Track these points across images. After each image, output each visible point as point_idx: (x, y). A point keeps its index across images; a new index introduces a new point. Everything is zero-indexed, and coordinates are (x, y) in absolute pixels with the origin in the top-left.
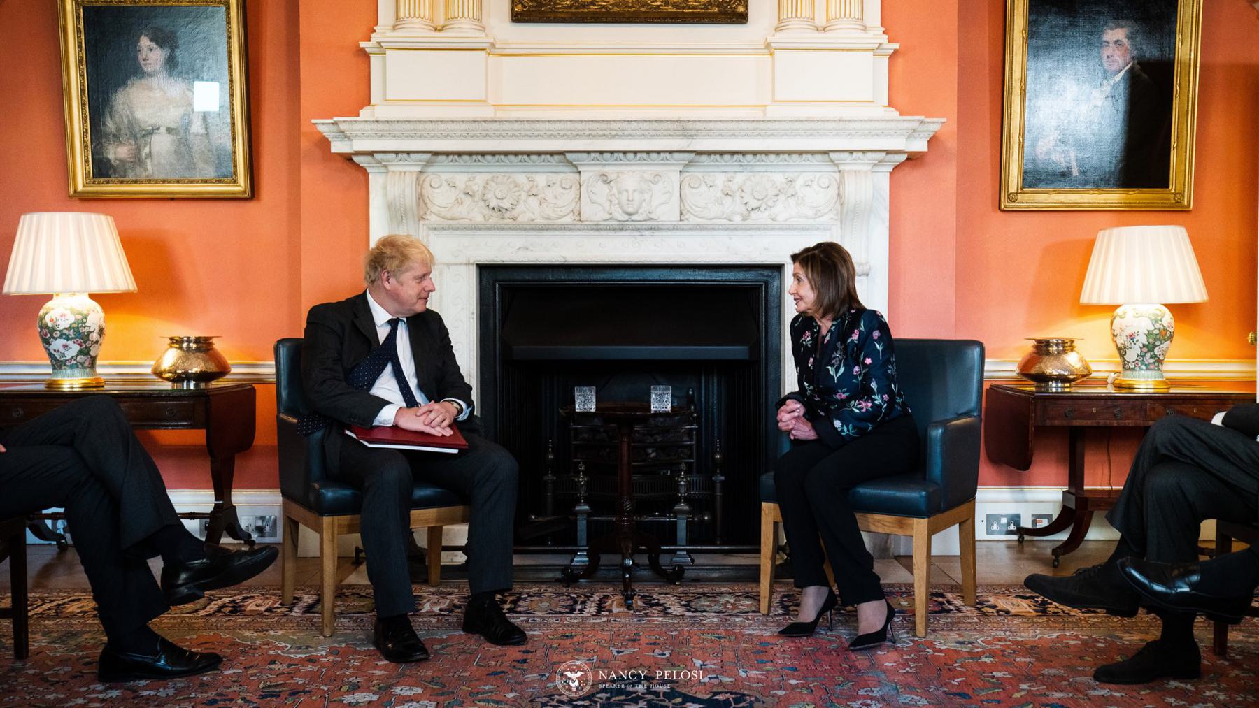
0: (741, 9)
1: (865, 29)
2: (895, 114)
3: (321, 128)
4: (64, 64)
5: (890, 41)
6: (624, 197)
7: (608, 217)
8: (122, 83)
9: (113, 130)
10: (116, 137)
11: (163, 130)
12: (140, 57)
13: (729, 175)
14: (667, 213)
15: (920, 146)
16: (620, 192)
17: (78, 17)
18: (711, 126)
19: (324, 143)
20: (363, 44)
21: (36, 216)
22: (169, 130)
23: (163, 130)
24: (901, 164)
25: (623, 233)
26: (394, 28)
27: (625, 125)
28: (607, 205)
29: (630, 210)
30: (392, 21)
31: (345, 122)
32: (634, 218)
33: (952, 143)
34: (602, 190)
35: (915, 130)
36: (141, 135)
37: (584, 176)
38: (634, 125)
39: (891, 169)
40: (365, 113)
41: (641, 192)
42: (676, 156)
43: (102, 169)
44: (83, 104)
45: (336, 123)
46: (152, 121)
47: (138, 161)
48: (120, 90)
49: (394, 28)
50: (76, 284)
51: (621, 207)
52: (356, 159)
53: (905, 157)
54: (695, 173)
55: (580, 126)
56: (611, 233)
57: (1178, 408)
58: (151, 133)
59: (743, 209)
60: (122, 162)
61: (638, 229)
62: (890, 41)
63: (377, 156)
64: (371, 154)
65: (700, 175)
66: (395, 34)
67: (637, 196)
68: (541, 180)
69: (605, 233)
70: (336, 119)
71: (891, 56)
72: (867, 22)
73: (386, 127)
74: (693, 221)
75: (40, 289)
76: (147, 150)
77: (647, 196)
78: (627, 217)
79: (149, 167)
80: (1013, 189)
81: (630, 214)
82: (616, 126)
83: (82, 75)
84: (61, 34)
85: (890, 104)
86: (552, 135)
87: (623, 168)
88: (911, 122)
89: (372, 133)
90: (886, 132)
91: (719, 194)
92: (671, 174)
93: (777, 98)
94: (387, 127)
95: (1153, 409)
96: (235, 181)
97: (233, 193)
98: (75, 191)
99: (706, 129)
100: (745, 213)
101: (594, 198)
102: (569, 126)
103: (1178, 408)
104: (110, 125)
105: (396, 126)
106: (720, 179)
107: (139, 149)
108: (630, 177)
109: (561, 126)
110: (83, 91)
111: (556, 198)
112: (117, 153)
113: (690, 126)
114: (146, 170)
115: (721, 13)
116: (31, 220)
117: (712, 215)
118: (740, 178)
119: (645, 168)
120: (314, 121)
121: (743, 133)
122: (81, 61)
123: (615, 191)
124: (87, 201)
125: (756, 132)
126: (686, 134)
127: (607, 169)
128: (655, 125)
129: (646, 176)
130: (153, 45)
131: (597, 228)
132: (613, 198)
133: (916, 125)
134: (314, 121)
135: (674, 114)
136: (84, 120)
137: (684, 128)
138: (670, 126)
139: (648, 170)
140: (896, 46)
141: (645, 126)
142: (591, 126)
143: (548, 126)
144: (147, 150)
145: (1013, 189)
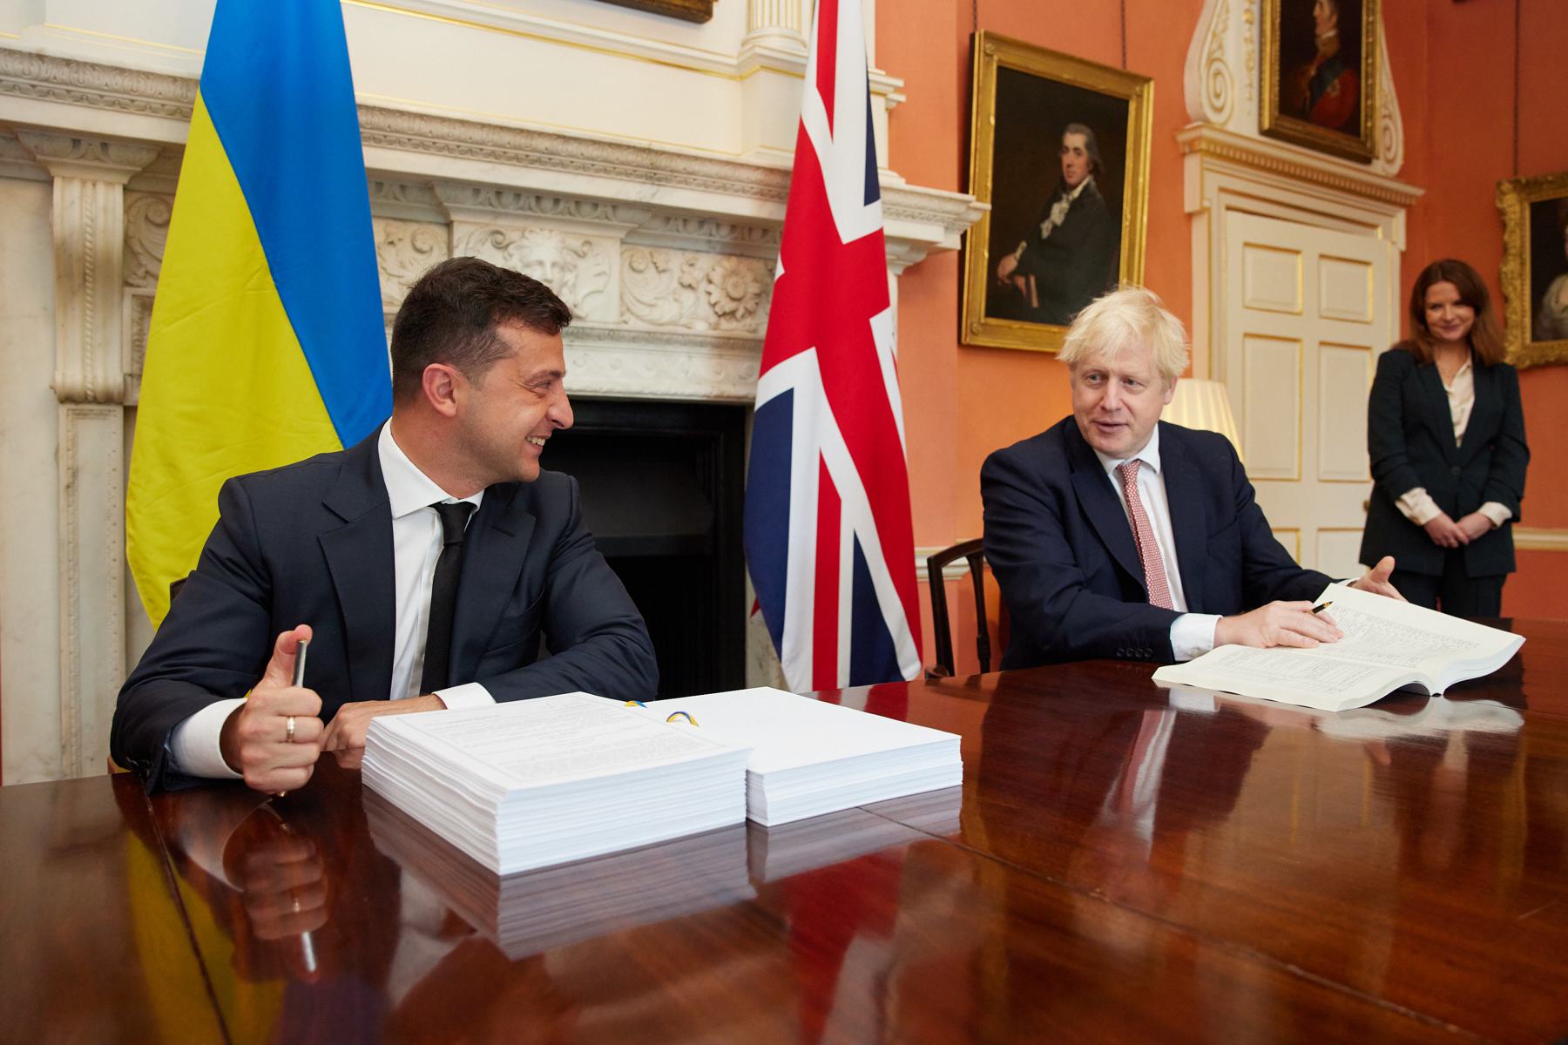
13: (689, 255)
18: (695, 166)
27: (558, 146)
38: (572, 148)
41: (563, 269)
65: (646, 251)
74: (634, 324)
77: (569, 277)
91: (675, 284)
100: (714, 319)
106: (675, 261)
113: (663, 161)
117: (665, 320)
126: (654, 175)
127: (502, 223)
137: (653, 163)
140: (902, 98)
143: (419, 125)
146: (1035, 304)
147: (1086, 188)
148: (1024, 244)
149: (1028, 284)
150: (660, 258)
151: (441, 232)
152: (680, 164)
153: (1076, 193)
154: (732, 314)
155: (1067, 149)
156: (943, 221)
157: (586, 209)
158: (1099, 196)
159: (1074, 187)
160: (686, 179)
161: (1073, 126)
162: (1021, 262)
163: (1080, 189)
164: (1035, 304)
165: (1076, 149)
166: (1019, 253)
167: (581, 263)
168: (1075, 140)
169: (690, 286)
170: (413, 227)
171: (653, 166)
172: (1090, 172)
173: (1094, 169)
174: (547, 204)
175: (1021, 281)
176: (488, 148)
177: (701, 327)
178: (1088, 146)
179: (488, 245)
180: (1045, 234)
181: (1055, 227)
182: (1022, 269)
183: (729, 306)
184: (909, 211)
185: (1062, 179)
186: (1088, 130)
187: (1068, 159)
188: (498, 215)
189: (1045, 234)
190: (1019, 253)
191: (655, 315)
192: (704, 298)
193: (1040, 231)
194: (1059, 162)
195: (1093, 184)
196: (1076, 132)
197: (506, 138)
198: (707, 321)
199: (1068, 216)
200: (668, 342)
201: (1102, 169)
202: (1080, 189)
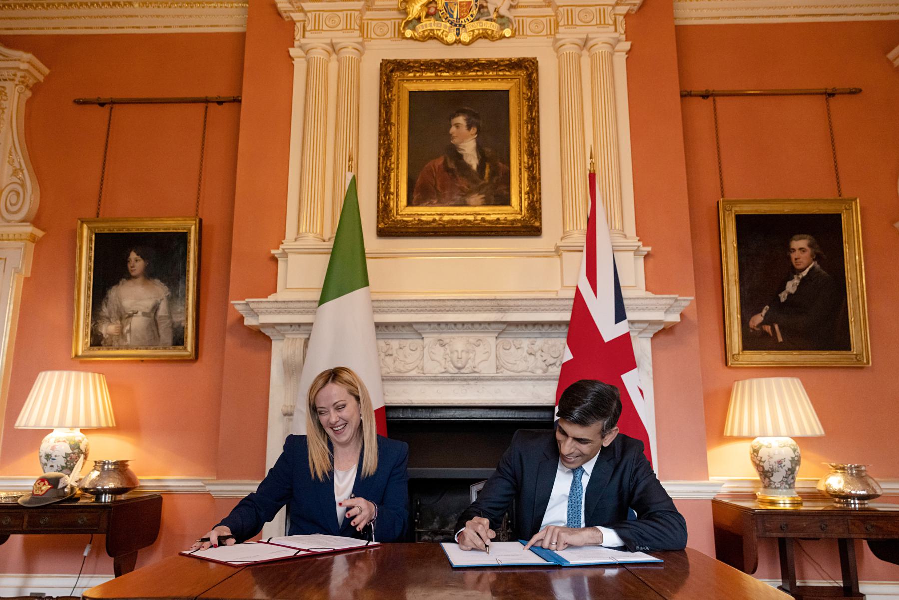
0: (537, 224)
1: (625, 236)
2: (650, 295)
3: (237, 307)
4: (77, 270)
5: (644, 245)
6: (455, 355)
7: (443, 370)
8: (115, 282)
9: (107, 314)
10: (109, 318)
11: (140, 313)
12: (129, 266)
13: (532, 340)
14: (487, 368)
15: (675, 318)
16: (452, 352)
17: (91, 240)
18: (520, 303)
19: (242, 319)
20: (273, 252)
21: (49, 373)
22: (144, 314)
23: (140, 313)
24: (659, 332)
25: (454, 382)
26: (296, 240)
27: (456, 303)
28: (443, 362)
29: (460, 365)
30: (294, 236)
31: (254, 302)
32: (462, 371)
33: (693, 317)
34: (439, 351)
35: (671, 306)
36: (124, 316)
37: (426, 341)
38: (462, 303)
39: (652, 336)
40: (271, 298)
41: (468, 352)
42: (494, 326)
43: (97, 340)
44: (89, 297)
45: (247, 304)
46: (135, 308)
47: (122, 334)
48: (114, 287)
49: (296, 240)
50: (69, 421)
51: (453, 363)
52: (263, 330)
53: (662, 327)
54: (508, 340)
55: (422, 304)
56: (446, 383)
57: (873, 523)
58: (130, 316)
59: (544, 365)
60: (111, 335)
61: (465, 380)
62: (644, 245)
63: (278, 328)
64: (273, 325)
65: (511, 340)
66: (297, 243)
67: (464, 355)
68: (395, 344)
69: (440, 382)
70: (247, 300)
71: (647, 257)
72: (627, 232)
73: (283, 305)
74: (507, 373)
75: (43, 425)
76: (128, 327)
77: (472, 355)
78: (457, 371)
79: (128, 339)
80: (736, 351)
81: (459, 368)
82: (448, 303)
83: (90, 278)
84: (78, 251)
85: (647, 290)
86: (402, 311)
87: (454, 335)
88: (666, 299)
89: (273, 310)
90: (650, 307)
91: (525, 354)
92: (490, 340)
93: (565, 284)
94: (285, 307)
95: (853, 524)
96: (185, 348)
97: (182, 356)
98: (77, 356)
99: (515, 306)
100: (545, 367)
101: (433, 357)
102: (415, 304)
103: (873, 523)
104: (105, 311)
105: (291, 305)
106: (525, 343)
107: (122, 328)
108: (459, 342)
109: (409, 304)
110: (89, 288)
111: (405, 357)
112: (108, 329)
113: (503, 303)
114: (126, 340)
115: (523, 227)
116: (69, 379)
117: (520, 369)
118: (540, 342)
119: (469, 335)
120: (232, 302)
121: (543, 308)
122: (90, 269)
123: (448, 351)
124: (80, 363)
125: (552, 308)
127: (443, 336)
128: (478, 303)
129: (471, 340)
130: (139, 258)
131: (435, 379)
132: (447, 357)
133: (672, 302)
134: (232, 302)
135: (492, 296)
136: (88, 308)
137: (500, 305)
138: (489, 303)
139: (473, 337)
140: (649, 249)
141: (470, 303)
142: (430, 303)
143: (399, 304)
144: (128, 327)
145: (736, 351)
146: (780, 339)
147: (813, 268)
148: (767, 307)
149: (773, 329)
150: (517, 342)
151: (420, 341)
152: (511, 303)
153: (804, 273)
154: (554, 364)
155: (794, 250)
156: (662, 309)
157: (477, 326)
158: (824, 272)
159: (804, 270)
160: (518, 309)
161: (795, 237)
162: (765, 317)
163: (807, 270)
164: (780, 339)
165: (800, 249)
166: (764, 312)
167: (476, 348)
168: (800, 244)
169: (531, 354)
170: (410, 341)
171: (499, 305)
172: (814, 260)
173: (817, 257)
174: (460, 326)
175: (768, 328)
176: (428, 309)
177: (539, 372)
178: (810, 246)
179: (437, 345)
180: (783, 300)
181: (790, 295)
182: (767, 321)
183: (552, 361)
184: (640, 307)
185: (793, 267)
186: (809, 237)
187: (793, 256)
188: (441, 333)
189: (783, 300)
190: (764, 312)
191: (515, 368)
192: (540, 359)
193: (779, 299)
194: (789, 258)
195: (818, 266)
196: (800, 239)
197: (434, 303)
198: (542, 368)
199: (799, 287)
200: (521, 380)
201: (824, 257)
202: (807, 270)
